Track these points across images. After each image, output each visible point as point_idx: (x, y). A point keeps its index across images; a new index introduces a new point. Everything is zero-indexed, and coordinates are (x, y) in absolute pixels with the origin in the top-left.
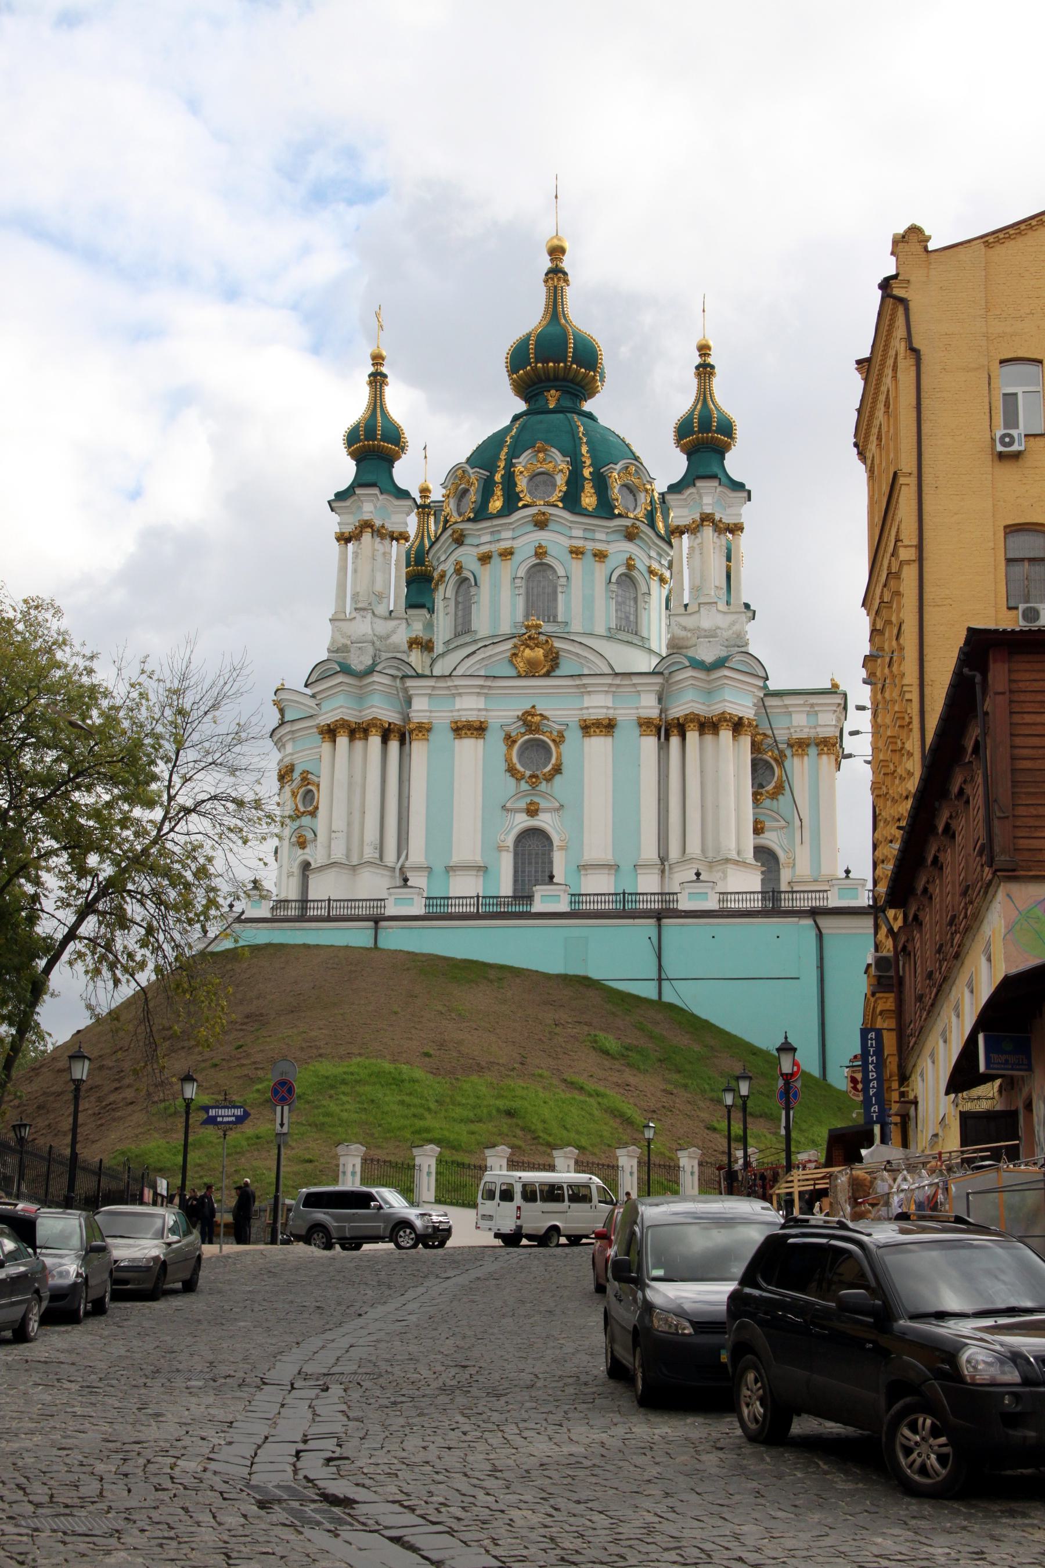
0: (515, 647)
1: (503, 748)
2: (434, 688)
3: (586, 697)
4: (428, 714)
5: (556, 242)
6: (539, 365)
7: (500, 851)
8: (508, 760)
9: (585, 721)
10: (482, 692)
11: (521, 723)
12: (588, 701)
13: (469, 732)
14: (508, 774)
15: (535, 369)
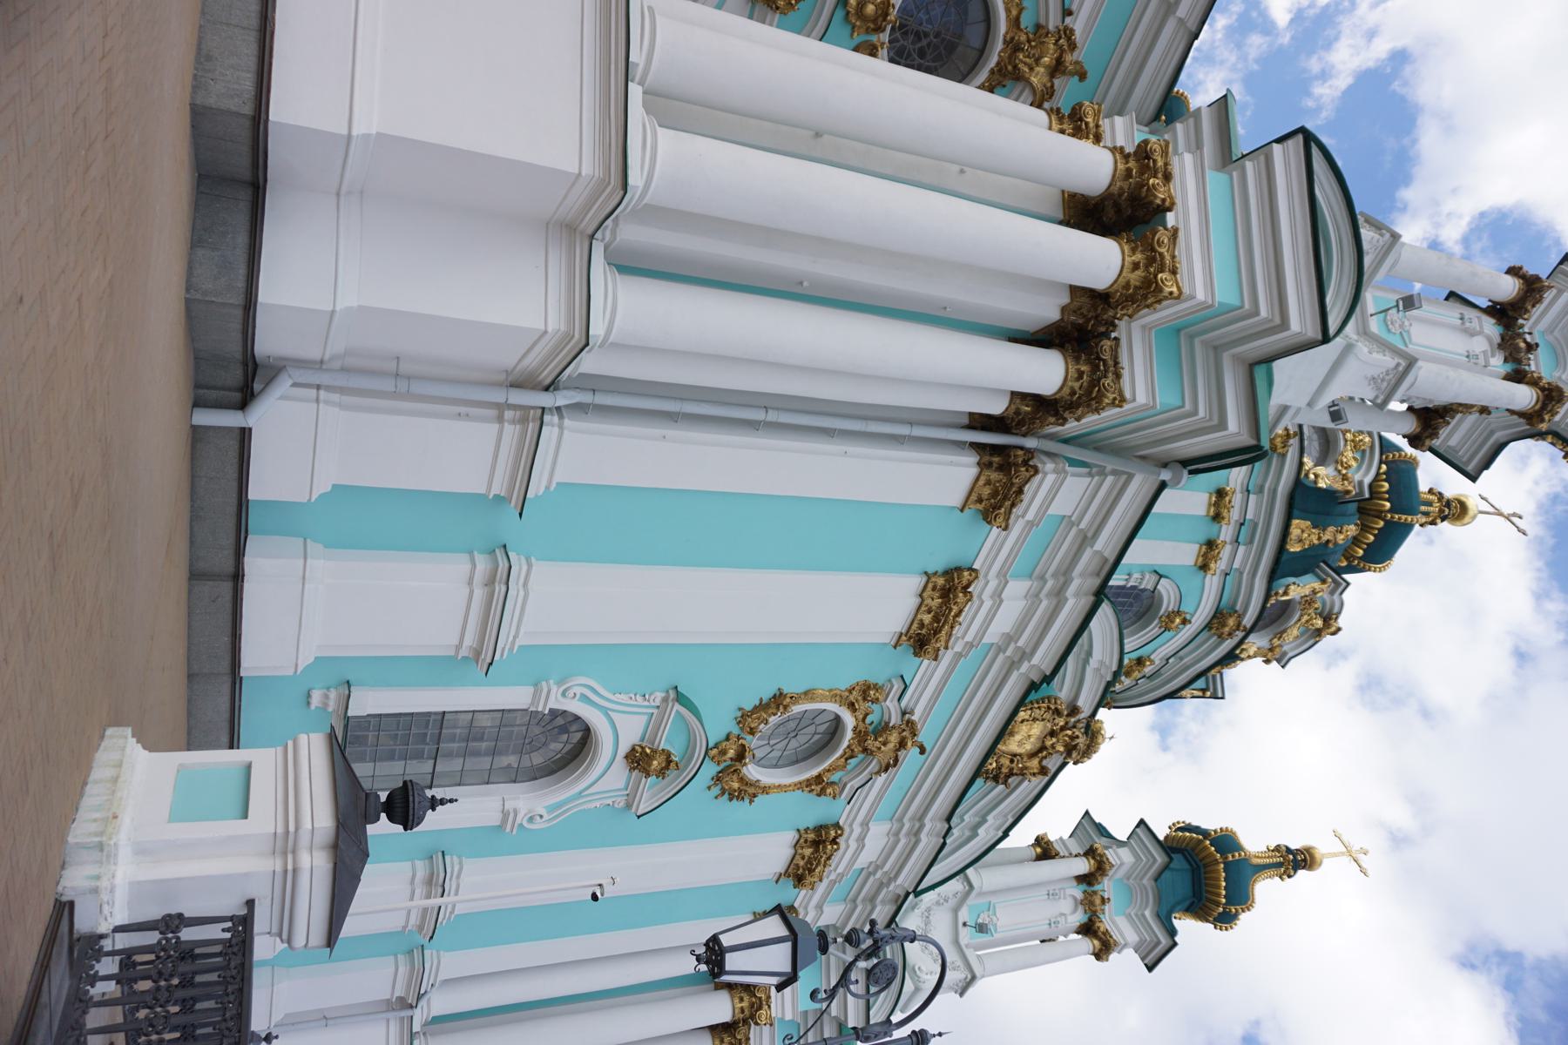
0: (1074, 710)
1: (843, 685)
2: (1085, 540)
3: (886, 826)
4: (1030, 516)
5: (1471, 513)
6: (1381, 524)
7: (536, 685)
8: (808, 695)
9: (834, 841)
10: (1012, 651)
11: (895, 720)
12: (878, 836)
13: (927, 618)
14: (767, 695)
15: (1379, 514)
